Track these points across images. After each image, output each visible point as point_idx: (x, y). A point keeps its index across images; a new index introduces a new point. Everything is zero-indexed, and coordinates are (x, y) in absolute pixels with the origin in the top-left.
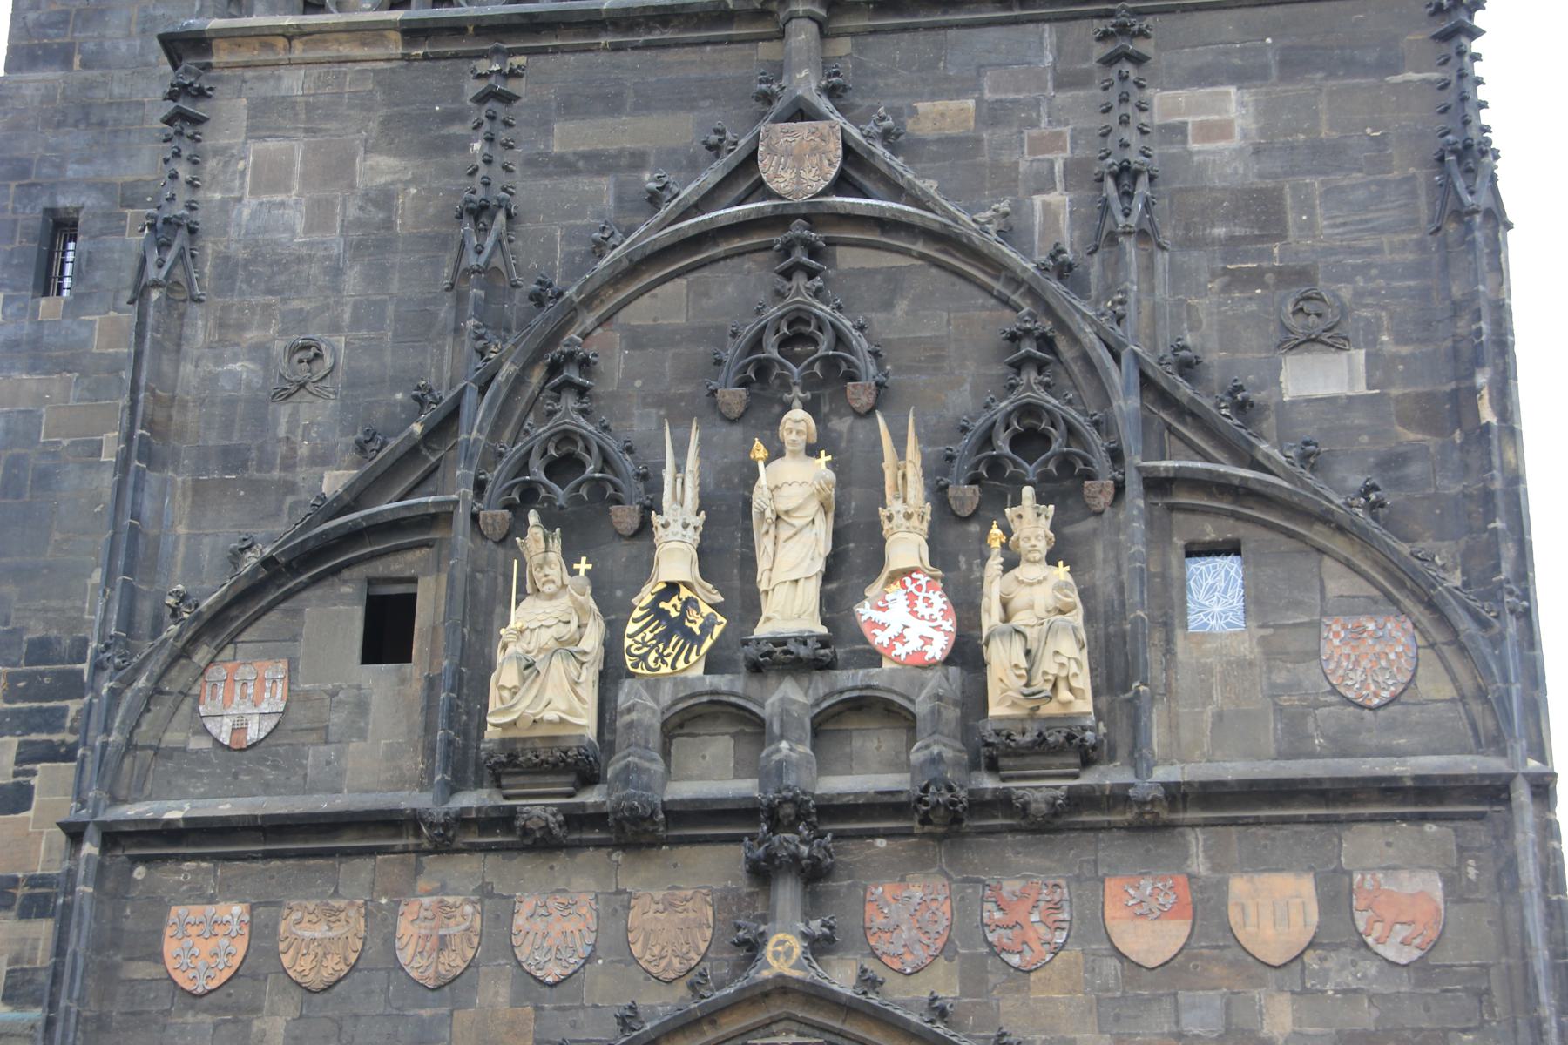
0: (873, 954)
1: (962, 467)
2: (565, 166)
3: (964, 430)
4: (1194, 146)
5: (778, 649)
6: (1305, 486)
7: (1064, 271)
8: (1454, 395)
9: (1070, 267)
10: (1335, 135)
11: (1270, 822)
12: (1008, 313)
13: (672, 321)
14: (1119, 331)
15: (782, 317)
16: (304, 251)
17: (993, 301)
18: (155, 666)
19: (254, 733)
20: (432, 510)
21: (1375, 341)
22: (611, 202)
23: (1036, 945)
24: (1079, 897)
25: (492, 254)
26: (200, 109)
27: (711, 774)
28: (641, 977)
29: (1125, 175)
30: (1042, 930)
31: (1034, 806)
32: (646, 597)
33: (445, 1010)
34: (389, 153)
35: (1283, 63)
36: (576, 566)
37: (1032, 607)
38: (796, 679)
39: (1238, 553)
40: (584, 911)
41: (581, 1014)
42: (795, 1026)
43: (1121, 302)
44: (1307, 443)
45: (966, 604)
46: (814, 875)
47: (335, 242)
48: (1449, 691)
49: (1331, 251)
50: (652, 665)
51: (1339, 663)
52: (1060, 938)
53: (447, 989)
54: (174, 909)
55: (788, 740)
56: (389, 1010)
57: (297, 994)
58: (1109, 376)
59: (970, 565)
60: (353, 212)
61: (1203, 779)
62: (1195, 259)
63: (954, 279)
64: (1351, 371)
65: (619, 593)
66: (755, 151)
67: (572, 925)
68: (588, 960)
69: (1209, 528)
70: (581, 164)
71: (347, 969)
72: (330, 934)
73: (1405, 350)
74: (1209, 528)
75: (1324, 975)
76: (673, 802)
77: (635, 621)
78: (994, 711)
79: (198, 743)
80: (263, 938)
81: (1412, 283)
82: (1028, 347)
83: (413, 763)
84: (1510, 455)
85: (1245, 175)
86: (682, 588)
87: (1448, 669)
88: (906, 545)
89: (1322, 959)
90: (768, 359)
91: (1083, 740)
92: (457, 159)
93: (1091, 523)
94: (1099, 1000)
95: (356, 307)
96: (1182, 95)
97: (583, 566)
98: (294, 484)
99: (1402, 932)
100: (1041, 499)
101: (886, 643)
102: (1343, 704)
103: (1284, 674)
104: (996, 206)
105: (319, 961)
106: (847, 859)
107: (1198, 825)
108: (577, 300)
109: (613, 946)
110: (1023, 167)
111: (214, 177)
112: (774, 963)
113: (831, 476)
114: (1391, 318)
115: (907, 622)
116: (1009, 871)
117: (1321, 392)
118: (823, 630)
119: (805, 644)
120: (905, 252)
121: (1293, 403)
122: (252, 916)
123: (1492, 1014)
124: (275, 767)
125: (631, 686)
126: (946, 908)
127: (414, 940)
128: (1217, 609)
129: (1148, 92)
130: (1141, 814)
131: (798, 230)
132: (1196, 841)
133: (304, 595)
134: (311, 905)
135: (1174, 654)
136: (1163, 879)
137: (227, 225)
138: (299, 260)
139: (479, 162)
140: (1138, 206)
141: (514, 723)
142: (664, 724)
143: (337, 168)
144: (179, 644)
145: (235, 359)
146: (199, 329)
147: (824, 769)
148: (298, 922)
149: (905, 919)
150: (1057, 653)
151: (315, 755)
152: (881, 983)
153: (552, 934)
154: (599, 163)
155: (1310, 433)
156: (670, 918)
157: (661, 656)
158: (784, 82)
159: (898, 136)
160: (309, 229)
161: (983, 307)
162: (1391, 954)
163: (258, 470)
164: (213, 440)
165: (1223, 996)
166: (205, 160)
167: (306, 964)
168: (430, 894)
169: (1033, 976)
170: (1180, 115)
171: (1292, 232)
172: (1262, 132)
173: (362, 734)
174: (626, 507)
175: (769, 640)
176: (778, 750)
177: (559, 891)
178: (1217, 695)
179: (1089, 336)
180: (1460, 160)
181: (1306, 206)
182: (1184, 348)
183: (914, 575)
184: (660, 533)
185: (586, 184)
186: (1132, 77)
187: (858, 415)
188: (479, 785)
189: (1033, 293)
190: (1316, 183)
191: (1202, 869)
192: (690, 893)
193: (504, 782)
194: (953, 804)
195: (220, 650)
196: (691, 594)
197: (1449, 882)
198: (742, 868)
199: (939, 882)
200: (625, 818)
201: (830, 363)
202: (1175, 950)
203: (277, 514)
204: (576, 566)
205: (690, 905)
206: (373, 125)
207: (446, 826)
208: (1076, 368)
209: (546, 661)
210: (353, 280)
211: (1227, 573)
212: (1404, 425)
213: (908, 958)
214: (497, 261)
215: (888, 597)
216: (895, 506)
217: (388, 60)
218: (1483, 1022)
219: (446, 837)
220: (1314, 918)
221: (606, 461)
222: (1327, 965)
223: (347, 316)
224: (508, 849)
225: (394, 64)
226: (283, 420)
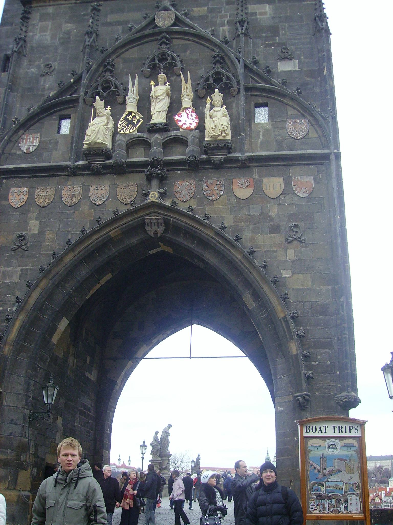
1: (201, 86)
2: (110, 24)
3: (202, 77)
4: (258, 17)
6: (283, 89)
7: (227, 42)
9: (228, 42)
12: (213, 52)
15: (159, 54)
17: (210, 50)
18: (10, 134)
19: (31, 150)
25: (92, 42)
26: (29, 16)
27: (139, 156)
28: (120, 203)
31: (216, 162)
32: (124, 116)
33: (73, 211)
37: (217, 117)
39: (267, 107)
40: (107, 188)
42: (156, 214)
46: (162, 179)
47: (57, 42)
48: (316, 136)
51: (291, 129)
53: (73, 207)
56: (60, 211)
57: (39, 208)
58: (237, 65)
60: (61, 36)
62: (258, 41)
63: (201, 46)
70: (114, 24)
73: (307, 60)
78: (206, 139)
79: (18, 152)
80: (31, 195)
84: (331, 83)
87: (316, 131)
88: (187, 102)
93: (233, 99)
96: (255, 6)
99: (304, 190)
100: (220, 91)
109: (113, 195)
115: (187, 120)
116: (209, 178)
121: (281, 72)
124: (36, 157)
128: (262, 119)
132: (255, 170)
135: (251, 128)
136: (247, 179)
139: (91, 24)
140: (244, 28)
142: (127, 145)
144: (15, 130)
145: (32, 68)
146: (25, 62)
147: (165, 155)
150: (222, 125)
151: (45, 154)
152: (177, 203)
154: (118, 23)
157: (127, 129)
158: (162, 3)
159: (188, 14)
160: (51, 39)
161: (208, 52)
162: (300, 195)
167: (41, 201)
169: (215, 202)
172: (274, 14)
173: (56, 150)
178: (261, 137)
179: (232, 56)
180: (319, 19)
182: (255, 58)
184: (127, 101)
185: (115, 28)
188: (83, 160)
189: (220, 48)
190: (286, 25)
195: (25, 131)
197: (315, 179)
199: (192, 181)
201: (170, 64)
206: (67, 18)
207: (74, 168)
208: (229, 64)
210: (60, 50)
214: (93, 44)
216: (184, 92)
217: (72, 4)
219: (74, 172)
221: (116, 87)
223: (58, 58)
225: (73, 5)
226: (42, 81)
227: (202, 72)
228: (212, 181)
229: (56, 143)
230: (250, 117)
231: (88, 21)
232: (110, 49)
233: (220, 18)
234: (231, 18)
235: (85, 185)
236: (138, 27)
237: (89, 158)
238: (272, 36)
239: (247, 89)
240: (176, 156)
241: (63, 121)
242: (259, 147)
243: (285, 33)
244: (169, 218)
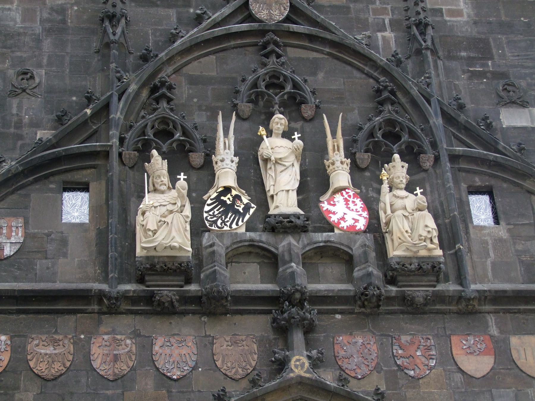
4: (448, 19)
5: (286, 220)
7: (399, 63)
11: (525, 312)
13: (210, 74)
15: (266, 74)
16: (22, 30)
17: (364, 76)
20: (99, 149)
22: (175, 20)
23: (421, 367)
24: (439, 344)
25: (120, 36)
28: (222, 377)
29: (422, 26)
30: (423, 359)
31: (417, 299)
33: (119, 391)
36: (178, 177)
38: (292, 236)
40: (190, 344)
41: (192, 395)
43: (428, 78)
44: (520, 144)
45: (372, 206)
46: (309, 329)
47: (38, 28)
49: (515, 66)
50: (220, 226)
52: (433, 363)
53: (119, 381)
57: (39, 382)
59: (367, 191)
60: (45, 15)
62: (454, 64)
67: (184, 351)
68: (194, 368)
69: (477, 179)
71: (65, 370)
74: (477, 179)
77: (209, 205)
82: (386, 94)
83: (92, 270)
90: (261, 92)
91: (440, 268)
93: (423, 175)
94: (454, 392)
95: (49, 57)
101: (336, 221)
103: (521, 246)
104: (365, 33)
105: (50, 364)
106: (322, 323)
107: (491, 313)
109: (207, 360)
110: (370, 20)
112: (296, 371)
113: (301, 142)
115: (346, 212)
119: (299, 218)
120: (321, 52)
121: (508, 128)
122: (11, 342)
124: (19, 269)
125: (209, 236)
127: (101, 356)
128: (483, 217)
130: (467, 306)
131: (270, 36)
132: (491, 320)
133: (30, 187)
135: (470, 235)
136: (479, 336)
138: (19, 34)
141: (155, 248)
148: (37, 345)
149: (356, 351)
150: (426, 226)
151: (40, 264)
153: (174, 355)
155: (519, 141)
156: (238, 348)
157: (223, 222)
160: (23, 21)
170: (440, 5)
171: (496, 57)
172: (476, 15)
173: (65, 255)
174: (197, 154)
175: (280, 215)
178: (492, 254)
179: (415, 91)
183: (347, 190)
187: (305, 120)
190: (503, 38)
193: (147, 278)
196: (237, 193)
199: (369, 336)
200: (214, 298)
202: (488, 369)
203: (14, 149)
204: (178, 177)
205: (244, 343)
207: (117, 299)
208: (408, 106)
209: (163, 219)
213: (358, 371)
214: (122, 40)
221: (185, 133)
223: (45, 61)
224: (147, 313)
226: (15, 106)
227: (355, 117)
228: (408, 338)
229: (64, 242)
233: (374, 14)
235: (139, 335)
236: (217, 16)
237: (151, 278)
238: (481, 59)
239: (454, 158)
240: (329, 282)
242: (490, 274)
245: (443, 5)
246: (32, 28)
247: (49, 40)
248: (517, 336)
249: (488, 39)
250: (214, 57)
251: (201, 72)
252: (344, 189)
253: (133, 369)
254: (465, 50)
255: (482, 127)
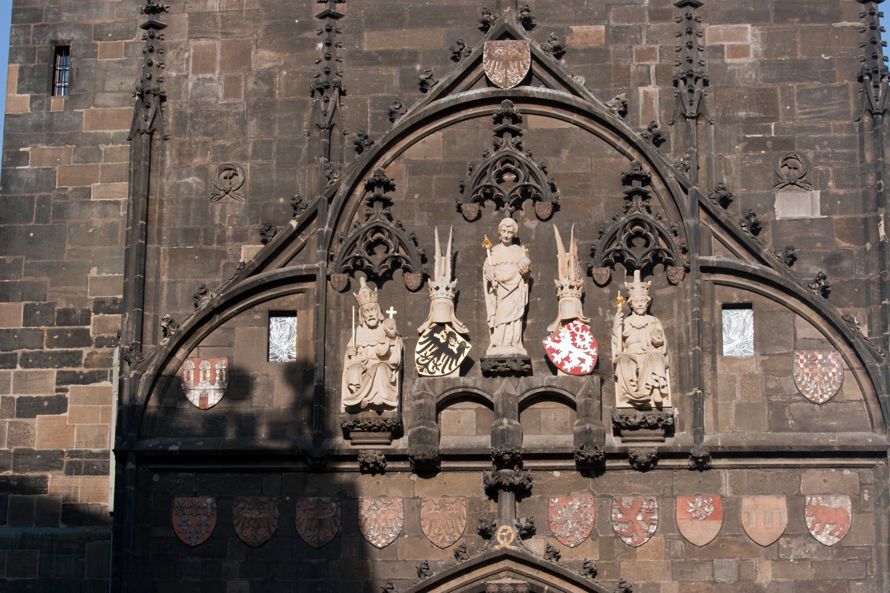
0: (553, 536)
4: (728, 60)
8: (865, 221)
10: (805, 57)
12: (625, 159)
14: (687, 175)
15: (497, 160)
16: (224, 109)
17: (617, 152)
20: (305, 273)
21: (826, 184)
24: (663, 506)
26: (161, 19)
32: (428, 331)
34: (270, 49)
35: (777, 11)
36: (387, 312)
41: (397, 565)
42: (511, 574)
43: (688, 159)
44: (788, 248)
46: (521, 492)
49: (801, 129)
50: (431, 370)
52: (653, 529)
54: (176, 499)
55: (507, 417)
59: (604, 313)
61: (731, 445)
64: (812, 204)
65: (409, 324)
66: (482, 56)
68: (399, 535)
69: (735, 295)
70: (380, 58)
72: (260, 516)
73: (841, 192)
74: (735, 295)
75: (789, 551)
76: (444, 450)
77: (421, 343)
80: (224, 514)
81: (845, 151)
85: (756, 79)
86: (447, 326)
87: (859, 383)
88: (570, 305)
89: (789, 543)
92: (309, 53)
94: (673, 564)
95: (254, 143)
96: (721, 28)
97: (391, 312)
98: (225, 252)
102: (805, 401)
104: (618, 96)
108: (381, 147)
109: (413, 529)
111: (171, 62)
112: (502, 542)
114: (834, 172)
115: (572, 350)
116: (625, 491)
117: (796, 215)
118: (524, 353)
121: (781, 221)
123: (872, 572)
126: (592, 511)
129: (702, 25)
133: (234, 319)
134: (249, 500)
136: (707, 498)
137: (180, 92)
138: (222, 114)
139: (322, 57)
142: (437, 404)
143: (240, 57)
144: (170, 349)
145: (189, 176)
148: (243, 509)
149: (569, 515)
154: (390, 58)
157: (436, 365)
160: (226, 96)
162: (822, 538)
163: (205, 243)
164: (179, 224)
165: (737, 562)
166: (166, 52)
168: (313, 495)
170: (722, 40)
172: (766, 53)
176: (502, 424)
177: (382, 496)
179: (671, 178)
181: (788, 101)
183: (575, 322)
184: (434, 293)
185: (383, 71)
186: (694, 17)
190: (794, 86)
191: (728, 492)
192: (453, 500)
193: (352, 435)
194: (597, 456)
195: (190, 351)
198: (482, 486)
203: (217, 270)
204: (387, 312)
206: (260, 31)
210: (252, 127)
211: (745, 320)
212: (841, 238)
215: (561, 335)
218: (867, 576)
220: (785, 520)
222: (791, 546)
223: (250, 150)
226: (217, 213)
227: (599, 213)
230: (711, 337)
231: (314, 42)
232: (379, 143)
233: (638, 60)
234: (664, 62)
236: (443, 81)
238: (763, 120)
240: (550, 429)
241: (274, 322)
243: (793, 115)
244: (539, 584)
245: (725, 40)
246: (235, 104)
247: (254, 121)
248: (751, 497)
249: (776, 89)
250: (441, 134)
251: (425, 157)
252: (571, 320)
253: (337, 536)
254: (744, 107)
255: (744, 229)
